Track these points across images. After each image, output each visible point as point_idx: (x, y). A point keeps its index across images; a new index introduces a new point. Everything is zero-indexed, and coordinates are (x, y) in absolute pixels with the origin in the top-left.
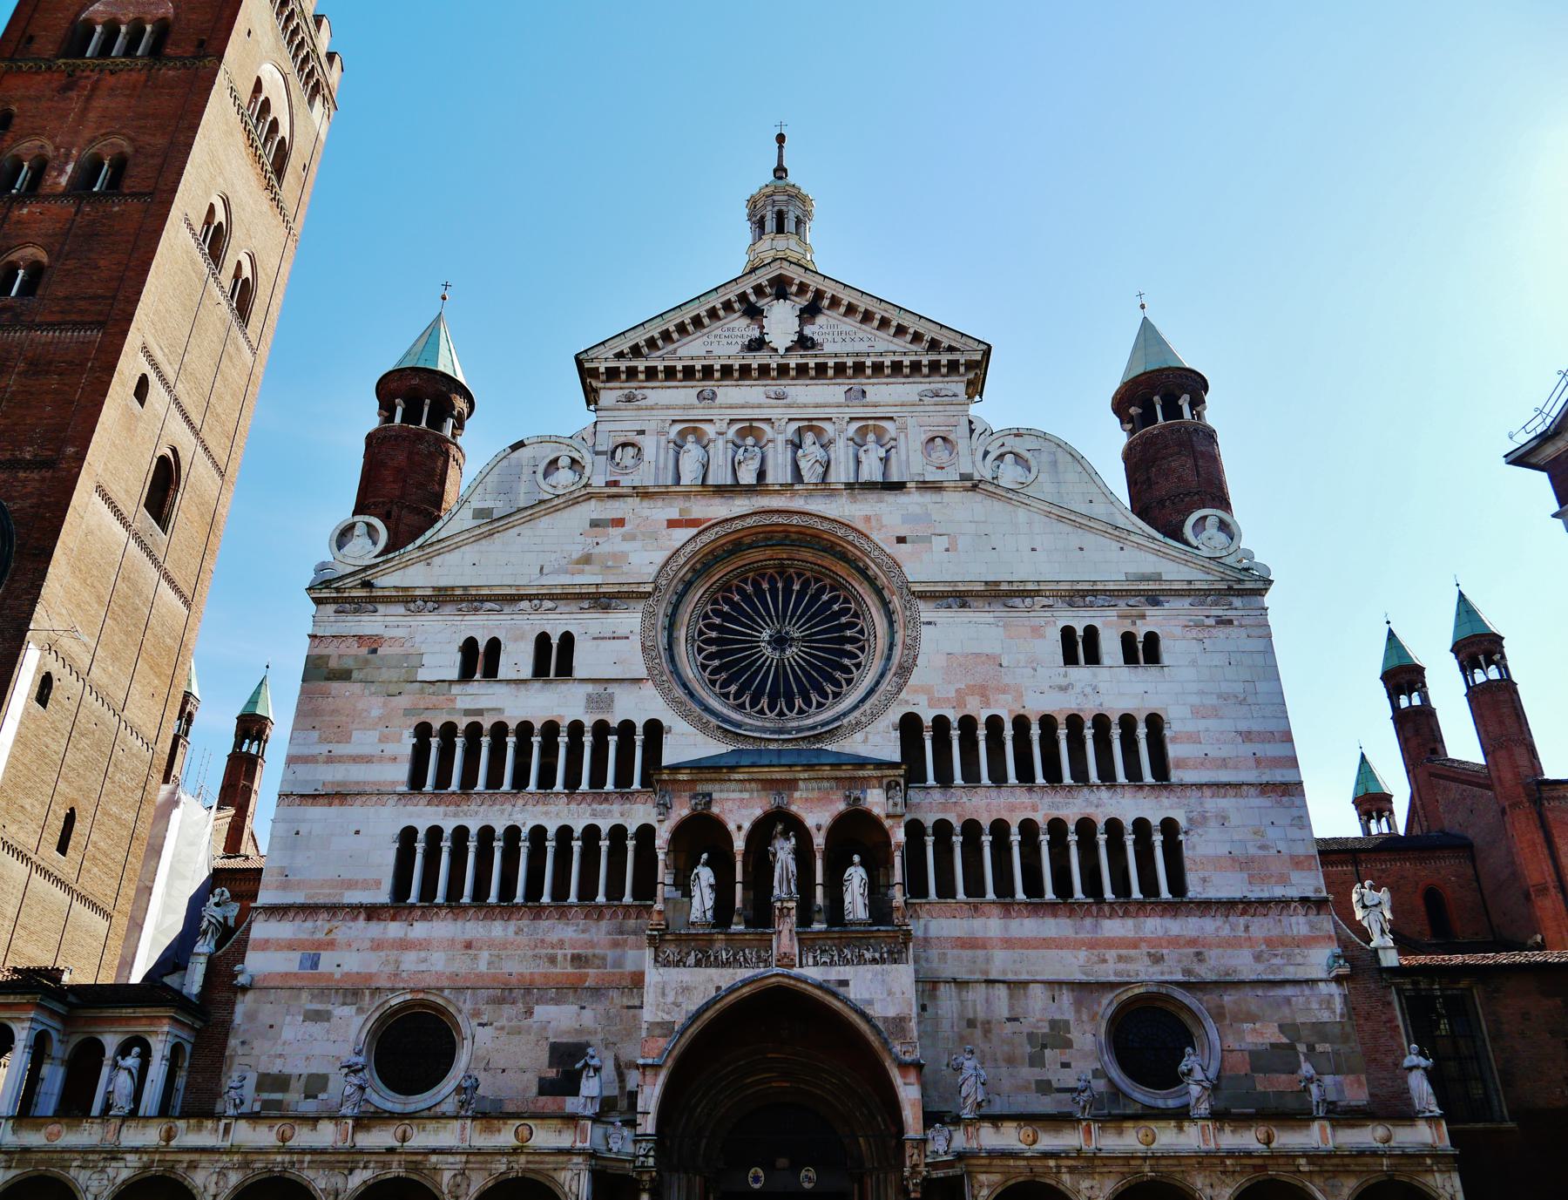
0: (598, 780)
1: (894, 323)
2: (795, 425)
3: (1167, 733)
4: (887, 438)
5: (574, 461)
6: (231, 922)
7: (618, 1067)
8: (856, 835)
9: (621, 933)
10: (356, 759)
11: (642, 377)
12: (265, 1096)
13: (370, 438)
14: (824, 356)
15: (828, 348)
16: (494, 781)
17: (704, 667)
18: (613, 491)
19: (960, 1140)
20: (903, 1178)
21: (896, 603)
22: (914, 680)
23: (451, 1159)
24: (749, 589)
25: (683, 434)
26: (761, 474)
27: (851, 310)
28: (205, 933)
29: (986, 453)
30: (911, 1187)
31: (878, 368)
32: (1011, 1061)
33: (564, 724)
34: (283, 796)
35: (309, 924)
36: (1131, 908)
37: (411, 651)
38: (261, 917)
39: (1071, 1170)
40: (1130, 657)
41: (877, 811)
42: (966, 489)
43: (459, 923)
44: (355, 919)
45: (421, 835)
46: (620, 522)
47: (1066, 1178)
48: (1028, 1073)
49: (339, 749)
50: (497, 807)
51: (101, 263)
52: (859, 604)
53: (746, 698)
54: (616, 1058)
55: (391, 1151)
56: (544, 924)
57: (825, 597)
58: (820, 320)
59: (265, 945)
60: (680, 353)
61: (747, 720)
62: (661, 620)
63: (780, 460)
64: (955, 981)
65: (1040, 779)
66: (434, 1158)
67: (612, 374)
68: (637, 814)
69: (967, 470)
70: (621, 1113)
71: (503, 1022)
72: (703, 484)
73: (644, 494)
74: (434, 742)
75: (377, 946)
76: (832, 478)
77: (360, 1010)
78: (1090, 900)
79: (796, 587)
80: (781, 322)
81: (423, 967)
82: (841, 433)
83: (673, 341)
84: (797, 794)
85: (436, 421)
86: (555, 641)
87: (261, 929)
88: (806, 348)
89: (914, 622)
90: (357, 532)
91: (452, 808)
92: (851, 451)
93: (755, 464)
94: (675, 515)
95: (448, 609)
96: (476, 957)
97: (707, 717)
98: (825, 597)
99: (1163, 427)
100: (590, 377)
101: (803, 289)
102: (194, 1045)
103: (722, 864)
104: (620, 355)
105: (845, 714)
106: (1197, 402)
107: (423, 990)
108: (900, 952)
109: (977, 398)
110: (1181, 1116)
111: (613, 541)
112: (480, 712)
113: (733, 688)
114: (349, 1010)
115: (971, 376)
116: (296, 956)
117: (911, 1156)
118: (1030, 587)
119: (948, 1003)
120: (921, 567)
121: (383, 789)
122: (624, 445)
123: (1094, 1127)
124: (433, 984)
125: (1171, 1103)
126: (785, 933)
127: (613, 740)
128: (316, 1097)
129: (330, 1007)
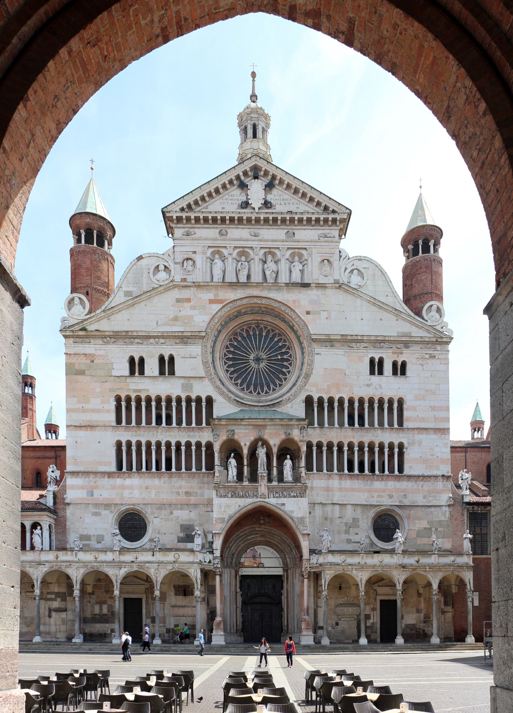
0: (189, 423)
1: (309, 196)
2: (263, 251)
3: (405, 406)
4: (303, 259)
6: (58, 478)
8: (288, 450)
9: (202, 483)
11: (193, 222)
13: (71, 250)
14: (276, 213)
15: (279, 208)
16: (149, 422)
17: (227, 371)
19: (321, 559)
20: (301, 571)
21: (305, 344)
22: (312, 380)
24: (245, 335)
26: (249, 277)
28: (50, 482)
29: (346, 269)
30: (304, 574)
32: (339, 532)
34: (67, 426)
36: (384, 477)
38: (69, 476)
39: (356, 569)
40: (395, 373)
41: (296, 438)
42: (336, 288)
43: (142, 479)
45: (124, 444)
47: (354, 572)
48: (344, 537)
54: (204, 530)
56: (174, 480)
58: (275, 191)
61: (245, 396)
62: (209, 350)
63: (257, 270)
64: (321, 503)
65: (356, 425)
68: (205, 436)
69: (337, 277)
70: (207, 549)
72: (223, 282)
74: (123, 404)
75: (114, 487)
76: (279, 281)
77: (111, 512)
78: (371, 474)
79: (264, 334)
80: (256, 190)
81: (131, 496)
82: (284, 255)
83: (206, 202)
85: (101, 244)
87: (70, 481)
88: (268, 208)
89: (312, 354)
90: (75, 303)
92: (288, 265)
93: (246, 272)
96: (150, 492)
97: (231, 395)
98: (276, 339)
99: (421, 257)
100: (171, 221)
101: (266, 173)
102: (55, 524)
105: (284, 395)
106: (437, 244)
107: (133, 505)
108: (303, 493)
109: (343, 237)
110: (392, 552)
114: (107, 512)
115: (342, 226)
117: (305, 564)
118: (359, 338)
119: (318, 510)
121: (106, 424)
123: (365, 556)
124: (136, 502)
125: (390, 547)
127: (193, 404)
129: (100, 511)
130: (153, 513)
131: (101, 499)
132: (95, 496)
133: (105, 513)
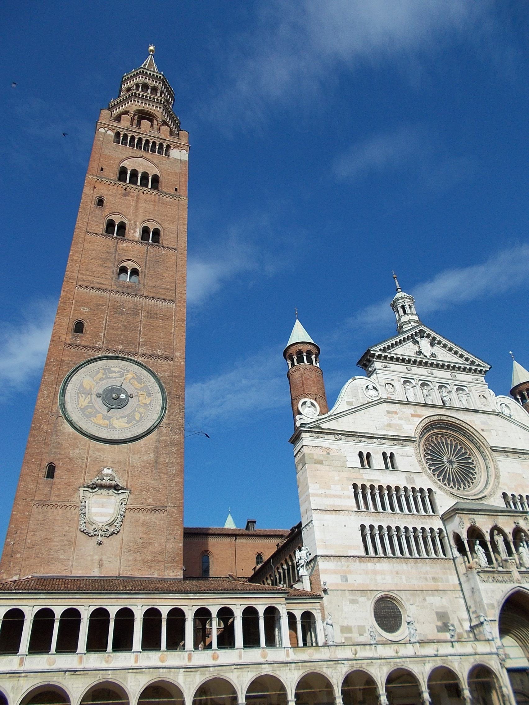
5: (374, 388)
7: (459, 621)
9: (445, 569)
10: (335, 496)
12: (345, 635)
18: (389, 401)
22: (502, 480)
23: (456, 657)
25: (405, 382)
27: (445, 346)
31: (459, 368)
33: (402, 487)
35: (339, 563)
37: (342, 455)
42: (495, 415)
44: (355, 561)
46: (396, 413)
49: (328, 492)
50: (390, 518)
51: (165, 275)
52: (470, 451)
53: (446, 482)
55: (436, 656)
57: (459, 447)
59: (326, 571)
60: (396, 352)
66: (450, 658)
67: (379, 357)
71: (418, 604)
73: (401, 403)
75: (366, 572)
81: (385, 581)
84: (499, 520)
86: (389, 455)
91: (375, 518)
94: (413, 413)
95: (350, 439)
96: (401, 578)
103: (484, 545)
104: (380, 350)
111: (395, 420)
112: (372, 481)
113: (441, 478)
116: (339, 576)
120: (493, 440)
122: (388, 384)
126: (514, 571)
128: (363, 635)
129: (357, 598)
130: (408, 600)
131: (356, 585)
132: (349, 583)
133: (362, 599)
